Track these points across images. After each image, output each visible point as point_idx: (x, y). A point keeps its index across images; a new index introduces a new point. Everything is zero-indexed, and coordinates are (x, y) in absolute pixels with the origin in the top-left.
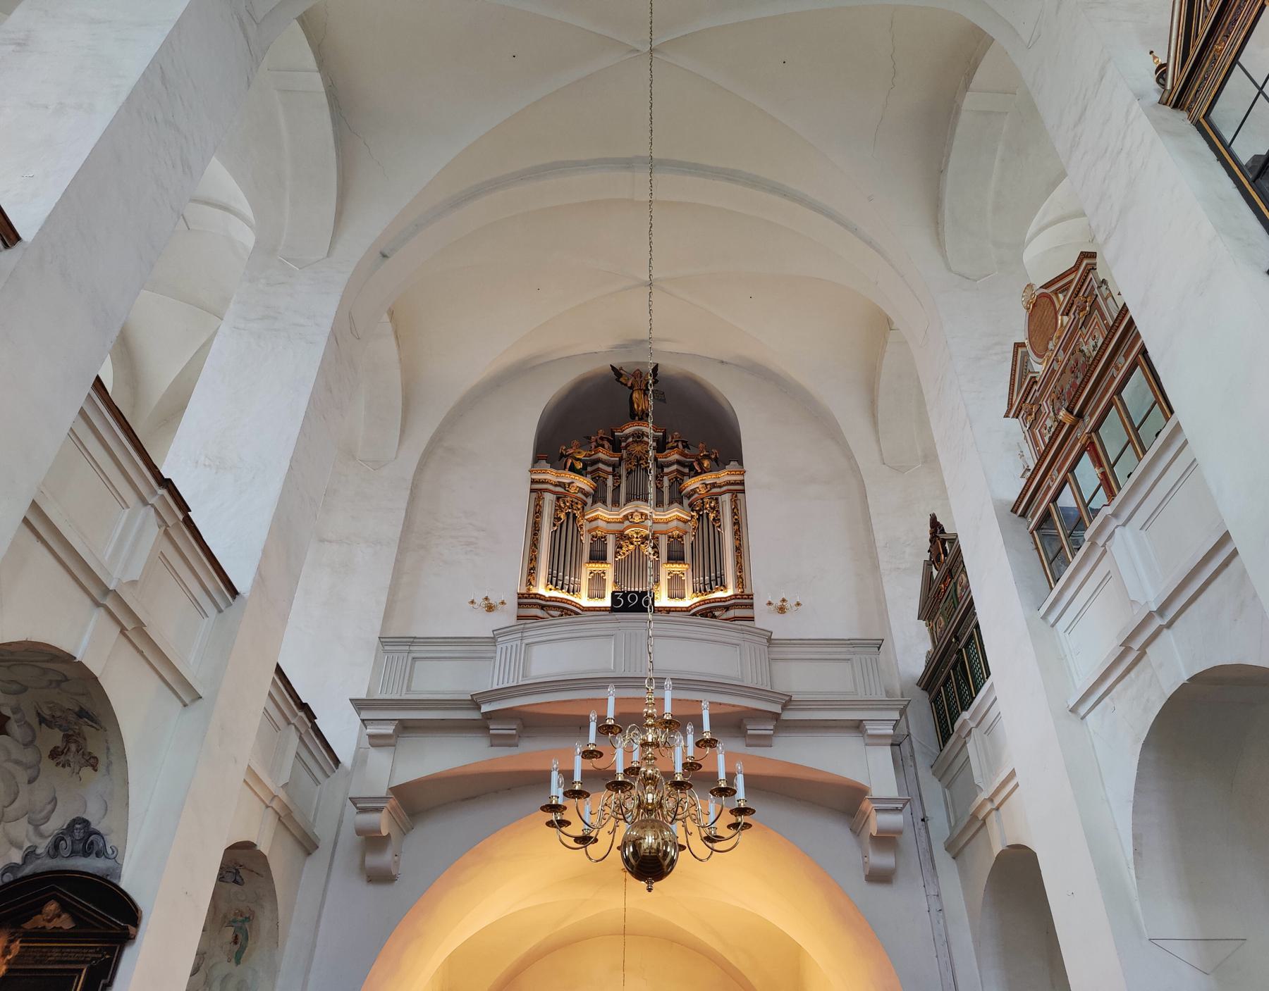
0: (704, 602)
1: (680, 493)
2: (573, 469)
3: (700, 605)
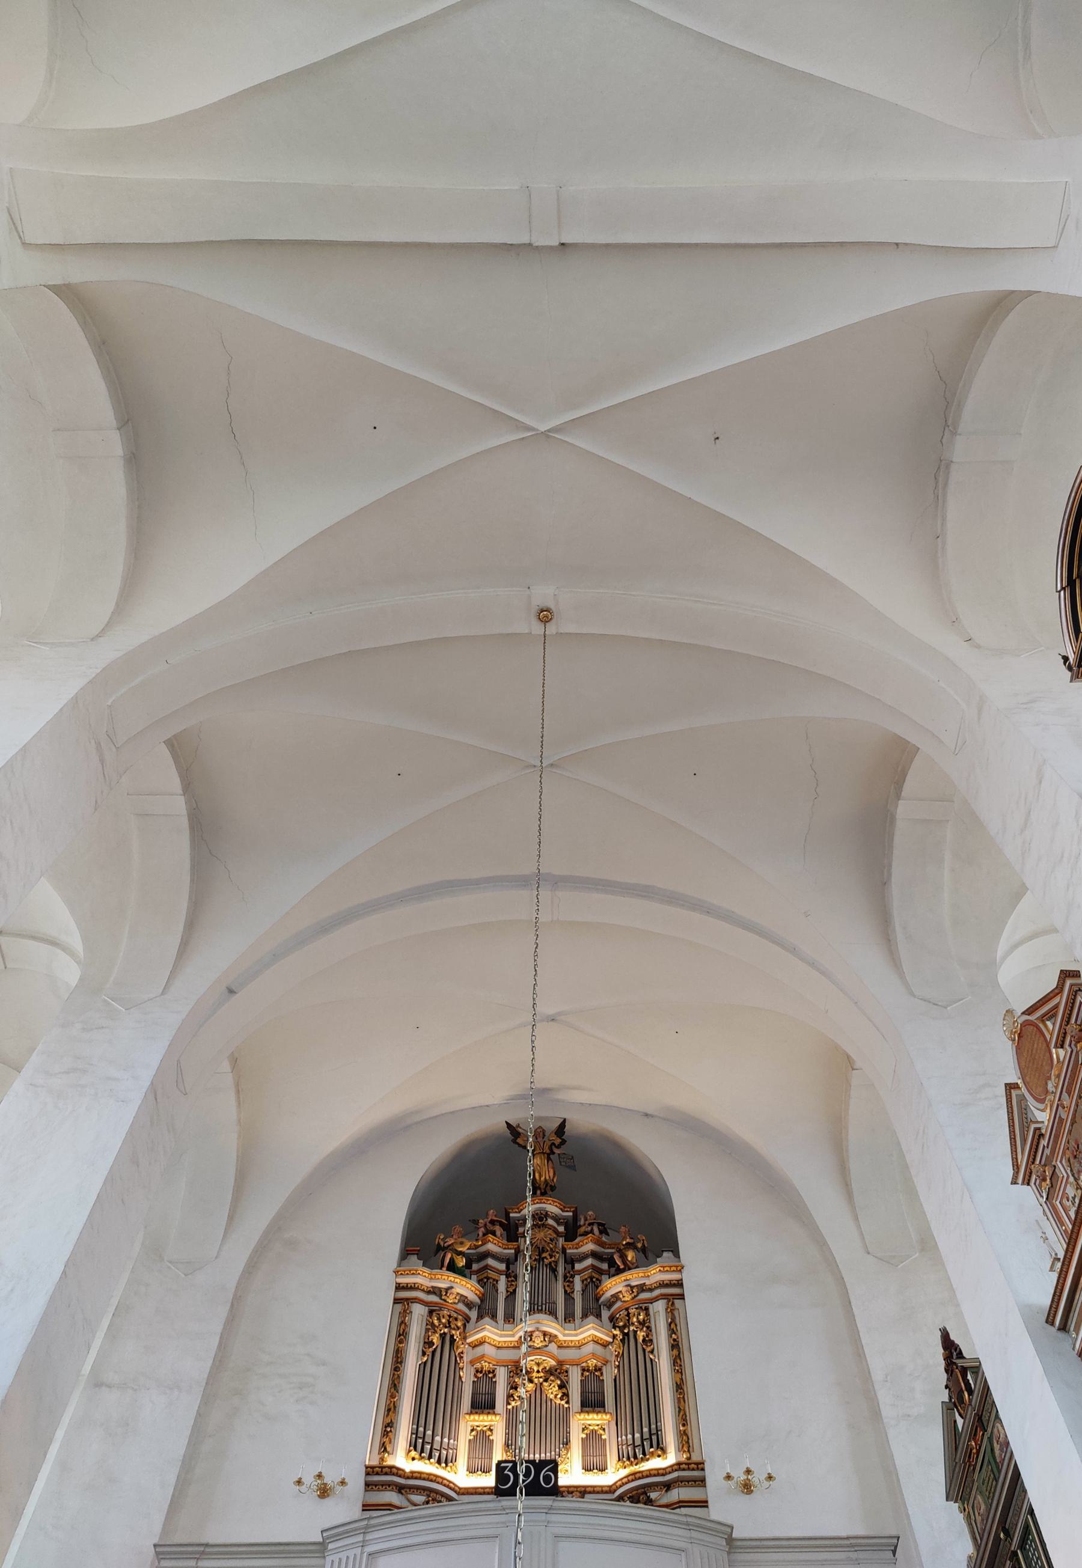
0: (635, 1476)
1: (598, 1300)
2: (452, 1268)
3: (629, 1482)
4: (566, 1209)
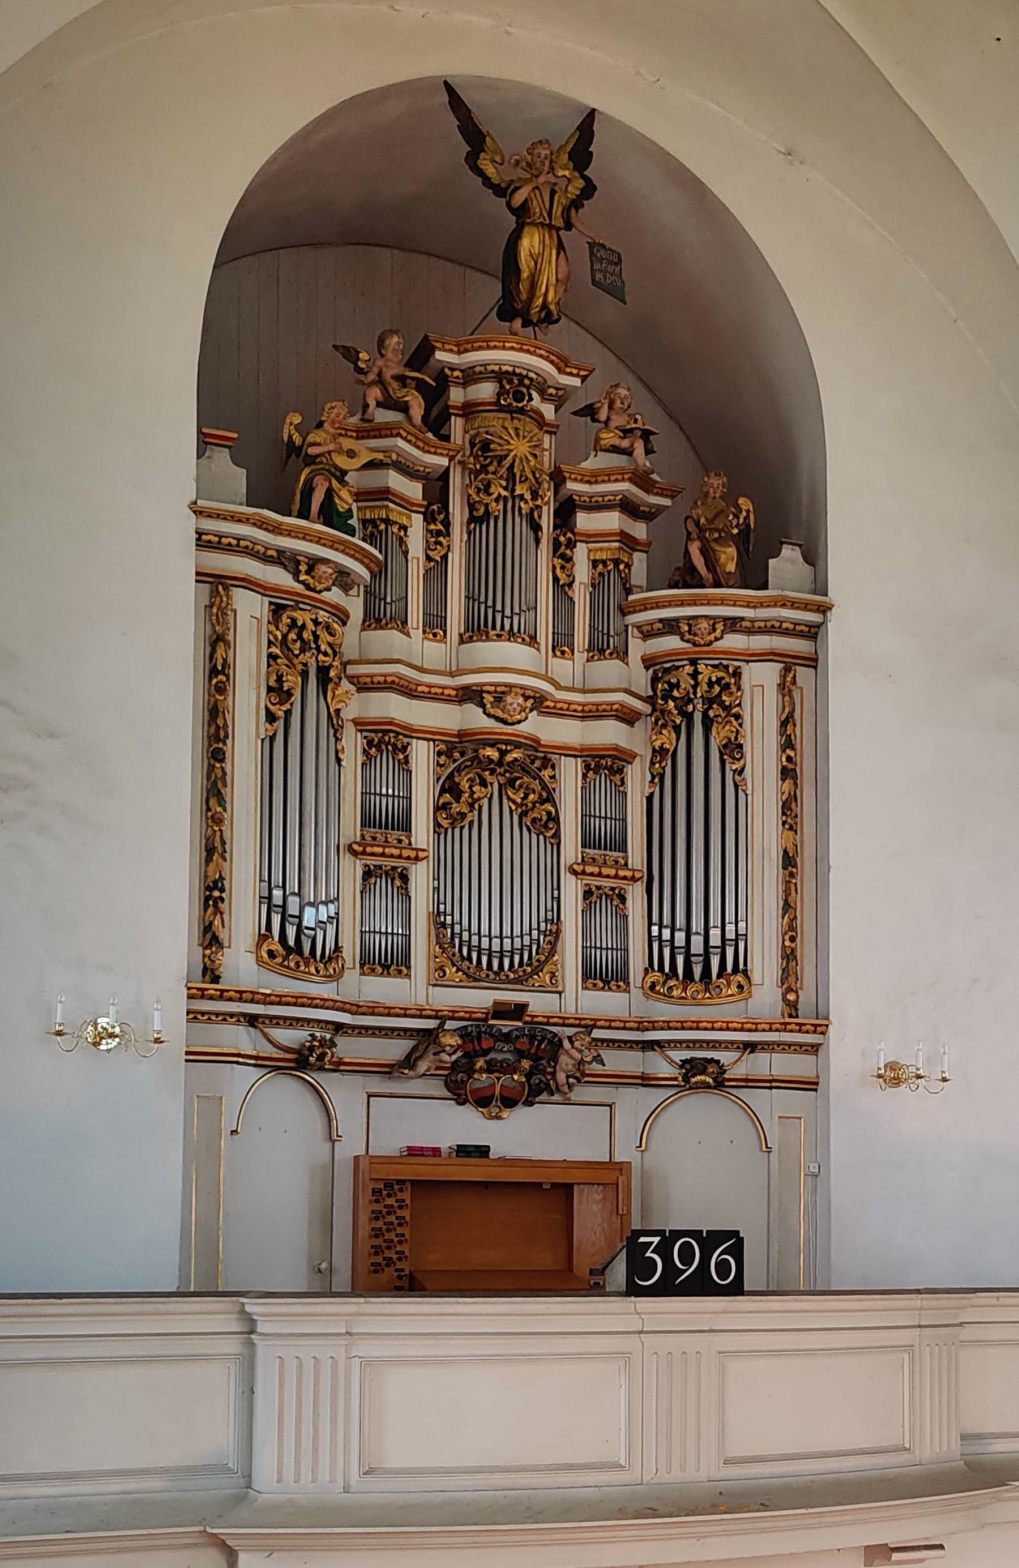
4: (568, 370)
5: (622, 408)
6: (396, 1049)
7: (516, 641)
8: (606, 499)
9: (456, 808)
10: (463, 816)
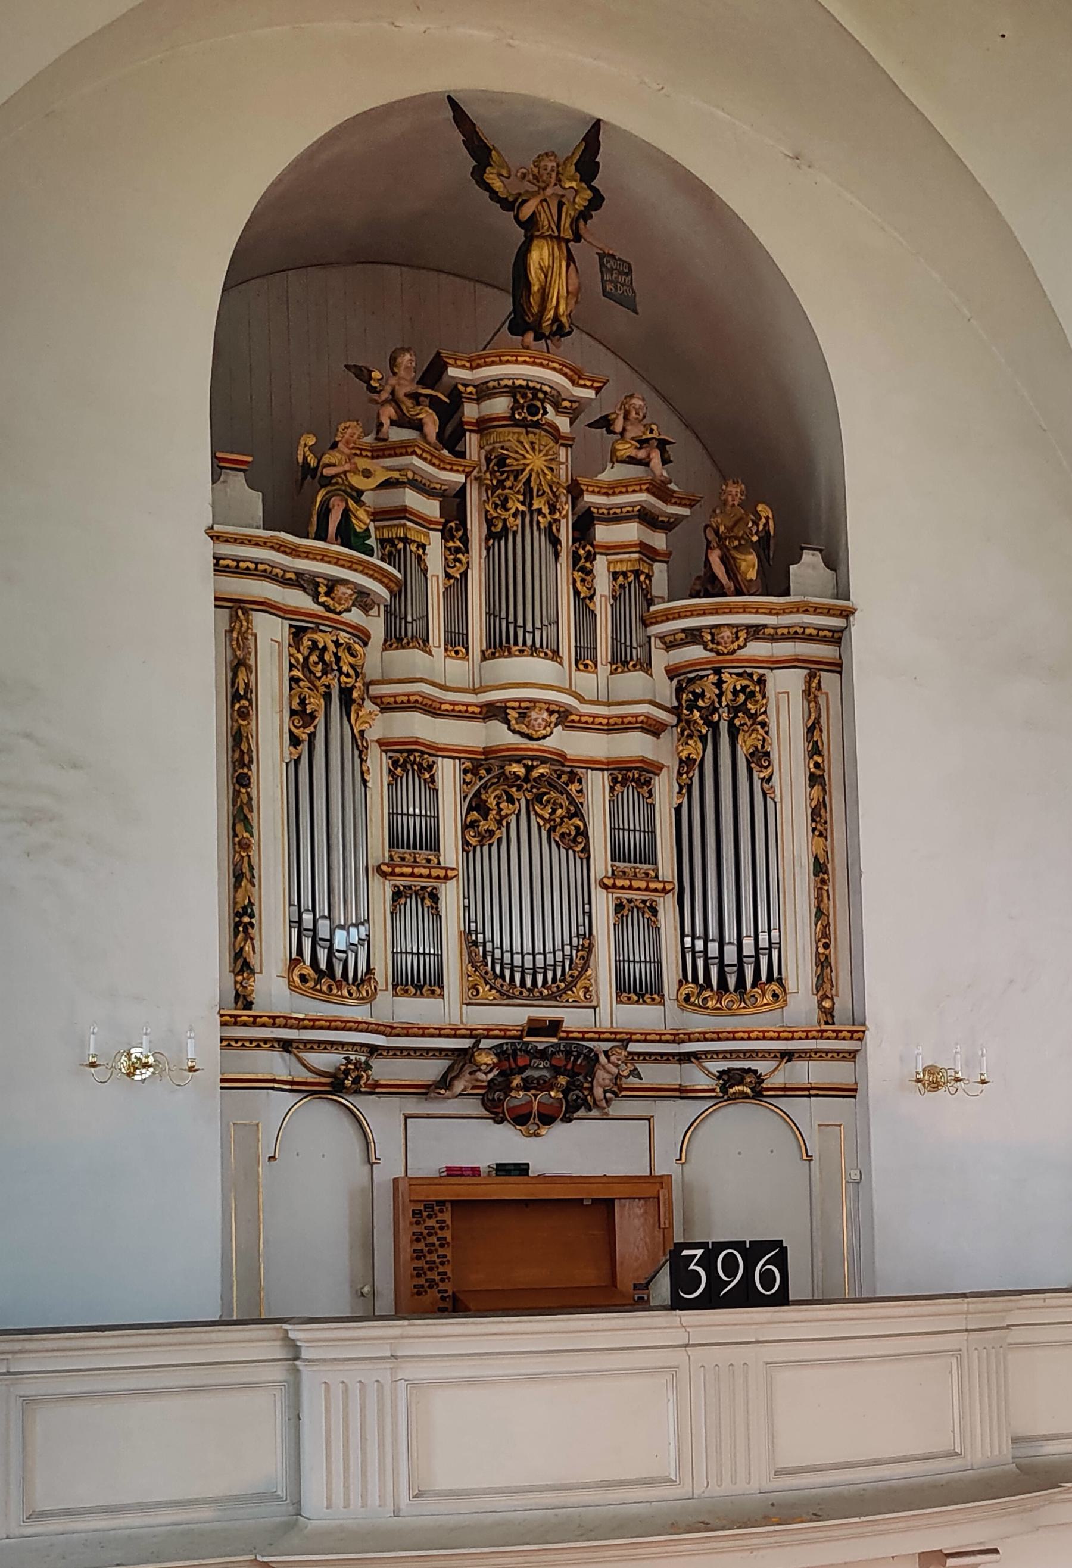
4: (582, 382)
5: (637, 419)
6: (432, 1070)
7: (538, 656)
8: (624, 510)
9: (484, 825)
10: (491, 833)
